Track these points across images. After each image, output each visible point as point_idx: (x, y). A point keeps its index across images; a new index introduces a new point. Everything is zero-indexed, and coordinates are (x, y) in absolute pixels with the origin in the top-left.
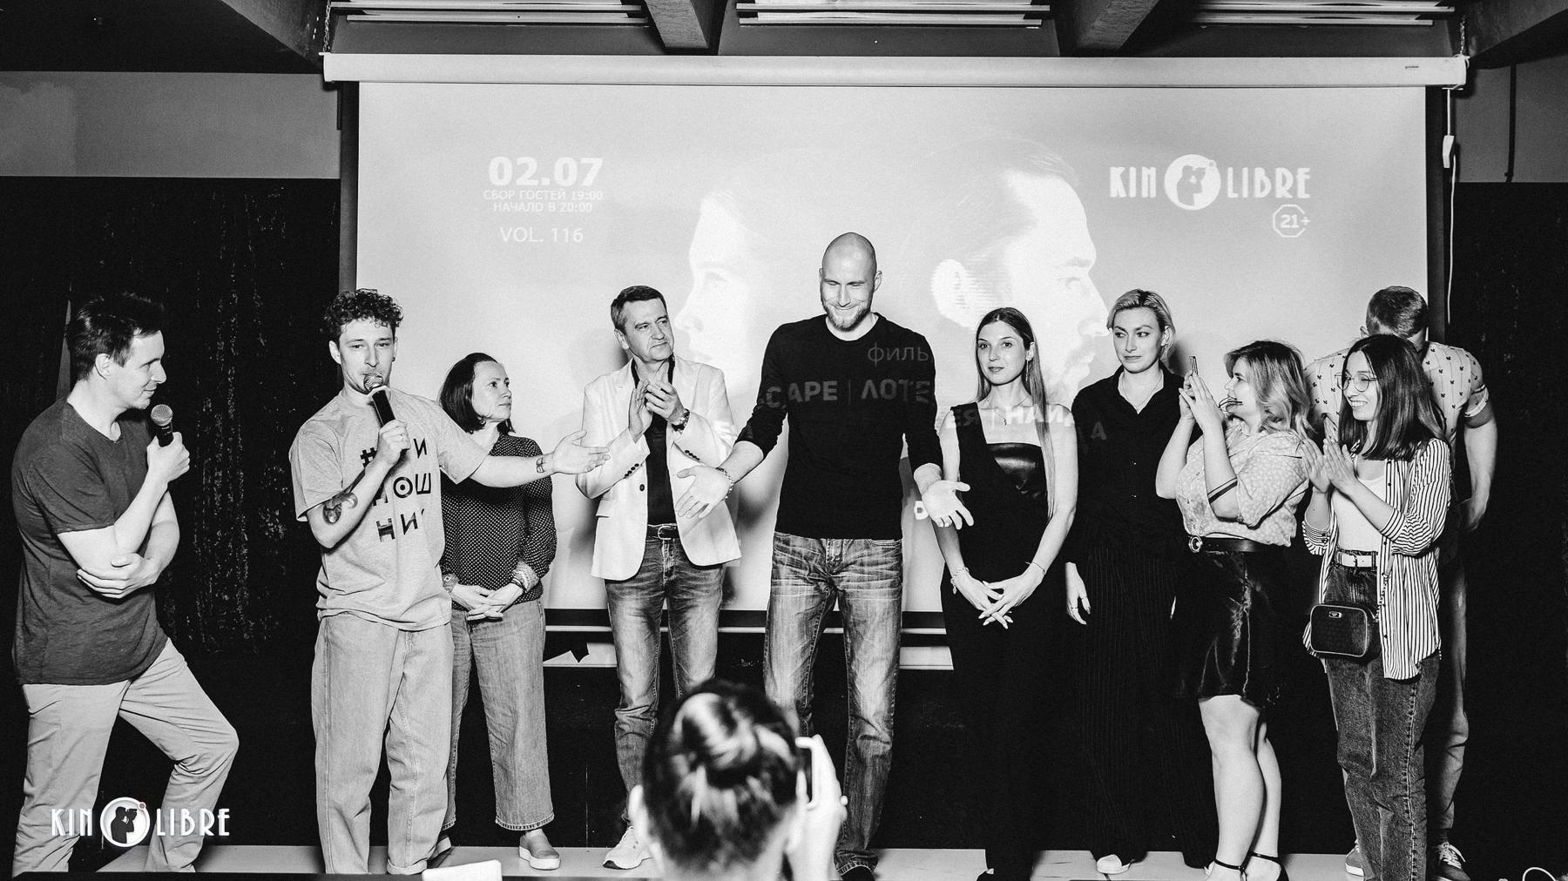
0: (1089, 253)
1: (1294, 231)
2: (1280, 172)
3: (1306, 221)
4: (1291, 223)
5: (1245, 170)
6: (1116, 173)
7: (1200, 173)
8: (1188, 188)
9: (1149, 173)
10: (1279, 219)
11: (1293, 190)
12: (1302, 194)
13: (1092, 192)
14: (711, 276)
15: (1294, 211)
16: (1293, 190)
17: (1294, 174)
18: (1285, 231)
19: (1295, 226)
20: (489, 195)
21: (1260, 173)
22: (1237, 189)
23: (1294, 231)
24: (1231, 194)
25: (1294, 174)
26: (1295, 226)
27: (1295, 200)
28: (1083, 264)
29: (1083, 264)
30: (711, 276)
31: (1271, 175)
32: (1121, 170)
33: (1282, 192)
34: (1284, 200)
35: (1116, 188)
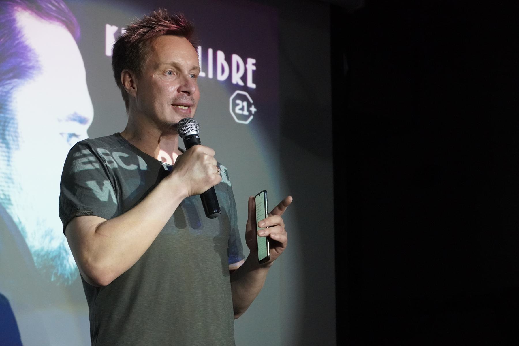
1: (246, 118)
2: (236, 58)
3: (253, 109)
4: (242, 109)
5: (210, 51)
10: (235, 105)
11: (244, 78)
12: (251, 84)
15: (243, 98)
17: (245, 63)
19: (246, 113)
21: (221, 55)
23: (246, 118)
25: (245, 63)
26: (246, 113)
27: (245, 88)
28: (82, 121)
29: (82, 121)
31: (229, 60)
33: (236, 79)
34: (237, 87)
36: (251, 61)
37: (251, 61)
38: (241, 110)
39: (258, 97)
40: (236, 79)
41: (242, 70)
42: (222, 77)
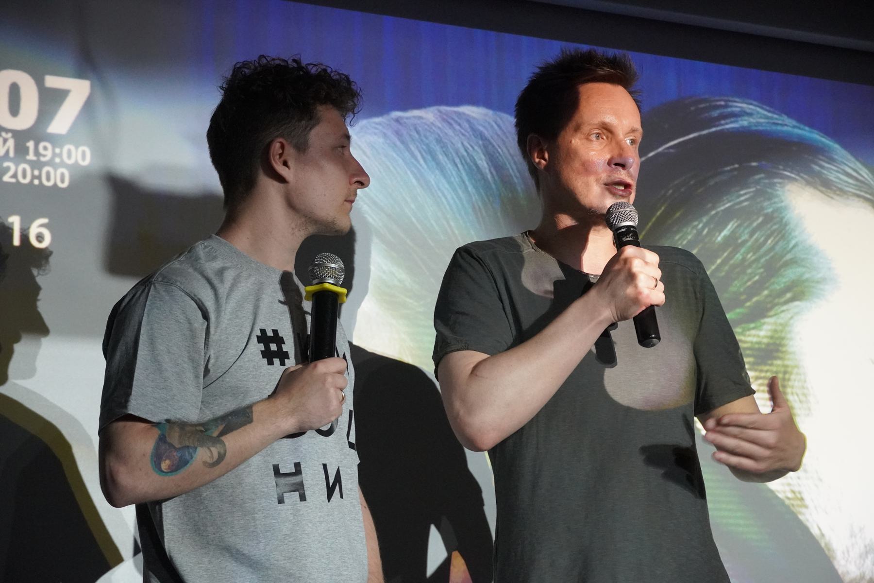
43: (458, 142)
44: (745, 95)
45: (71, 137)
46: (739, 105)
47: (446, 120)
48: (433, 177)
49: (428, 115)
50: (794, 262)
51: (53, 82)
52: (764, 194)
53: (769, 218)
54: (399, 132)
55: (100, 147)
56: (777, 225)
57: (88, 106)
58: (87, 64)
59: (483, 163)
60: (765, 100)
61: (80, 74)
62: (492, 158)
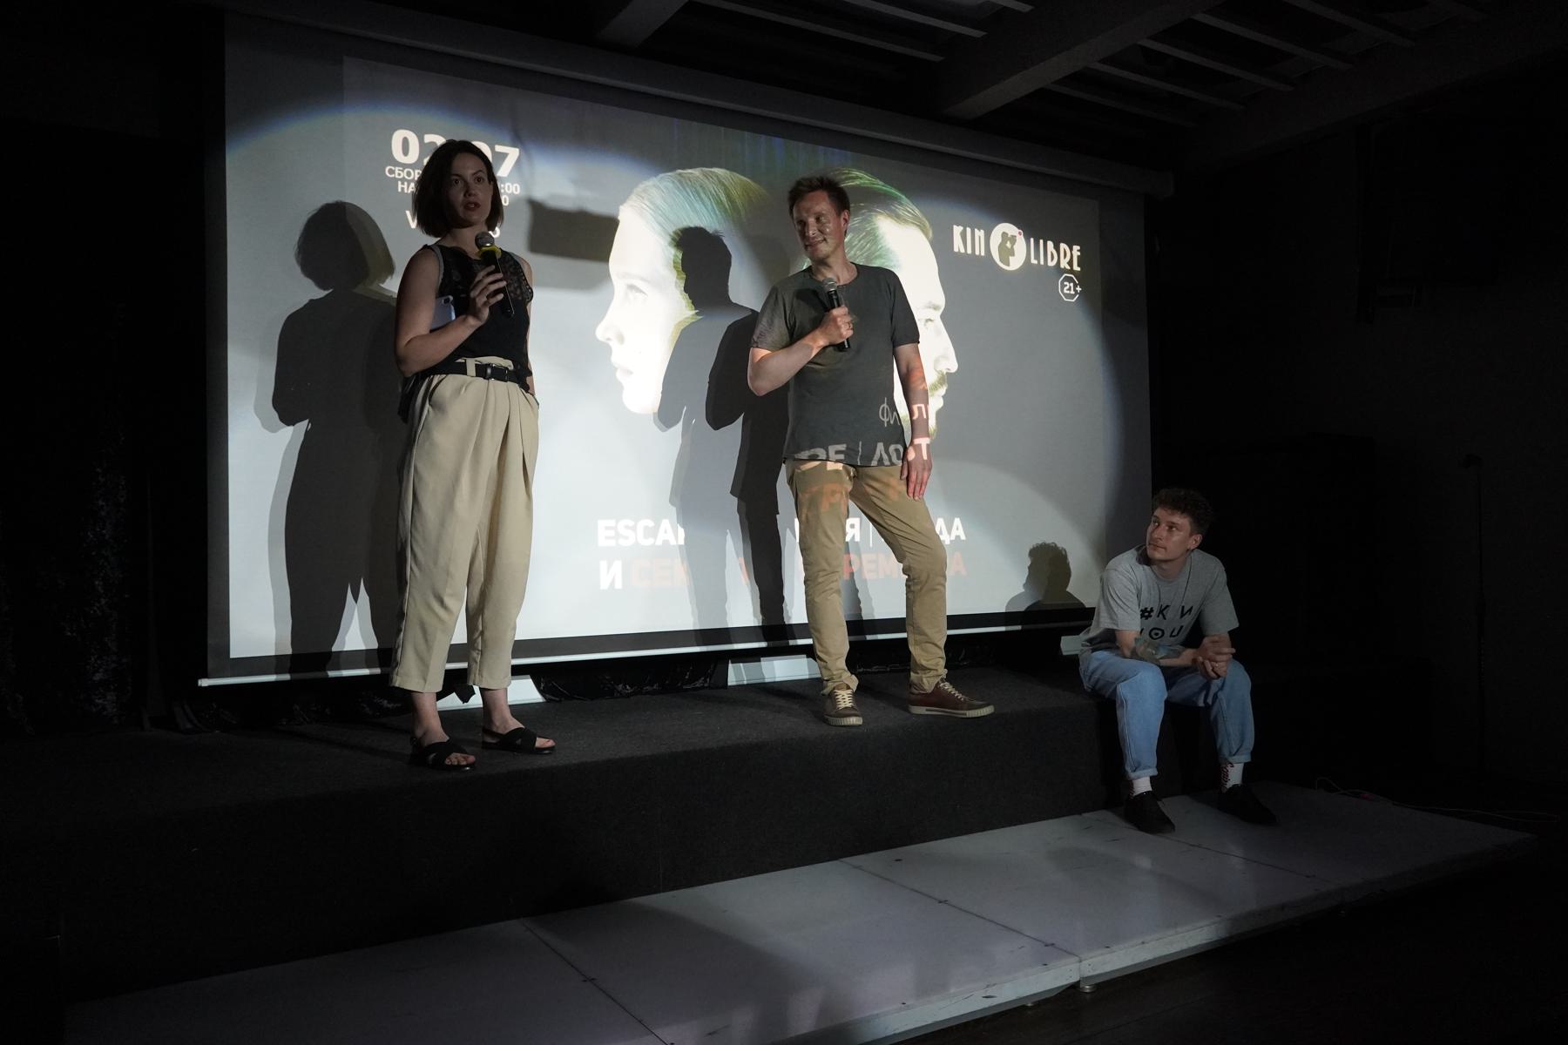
0: (941, 300)
1: (1072, 296)
2: (1063, 246)
6: (957, 230)
7: (1013, 240)
8: (1006, 253)
9: (980, 234)
10: (1063, 286)
11: (1070, 263)
12: (1076, 268)
13: (941, 246)
14: (632, 287)
15: (1070, 280)
16: (1070, 263)
18: (1068, 296)
20: (391, 172)
21: (1050, 244)
22: (1037, 257)
23: (1072, 296)
24: (1034, 261)
27: (1071, 271)
28: (936, 308)
29: (936, 308)
30: (632, 287)
31: (1057, 248)
32: (961, 228)
33: (1064, 264)
34: (1065, 271)
35: (958, 245)
36: (1076, 248)
37: (1076, 248)
38: (1069, 290)
39: (1082, 278)
40: (1064, 264)
41: (1069, 256)
42: (1051, 264)
43: (711, 187)
44: (859, 168)
45: (510, 178)
46: (856, 173)
47: (705, 175)
48: (698, 206)
49: (696, 172)
50: (880, 256)
51: (499, 148)
52: (867, 221)
53: (868, 233)
54: (682, 181)
55: (525, 184)
56: (873, 237)
57: (518, 162)
58: (517, 140)
59: (724, 198)
60: (866, 171)
61: (514, 146)
62: (728, 196)
